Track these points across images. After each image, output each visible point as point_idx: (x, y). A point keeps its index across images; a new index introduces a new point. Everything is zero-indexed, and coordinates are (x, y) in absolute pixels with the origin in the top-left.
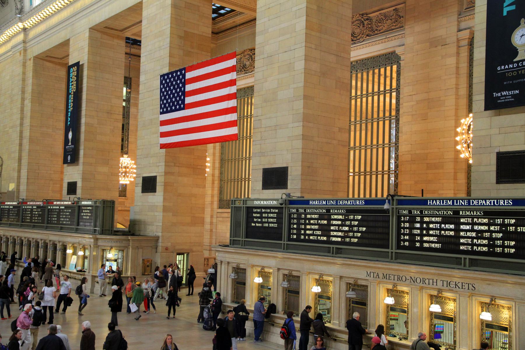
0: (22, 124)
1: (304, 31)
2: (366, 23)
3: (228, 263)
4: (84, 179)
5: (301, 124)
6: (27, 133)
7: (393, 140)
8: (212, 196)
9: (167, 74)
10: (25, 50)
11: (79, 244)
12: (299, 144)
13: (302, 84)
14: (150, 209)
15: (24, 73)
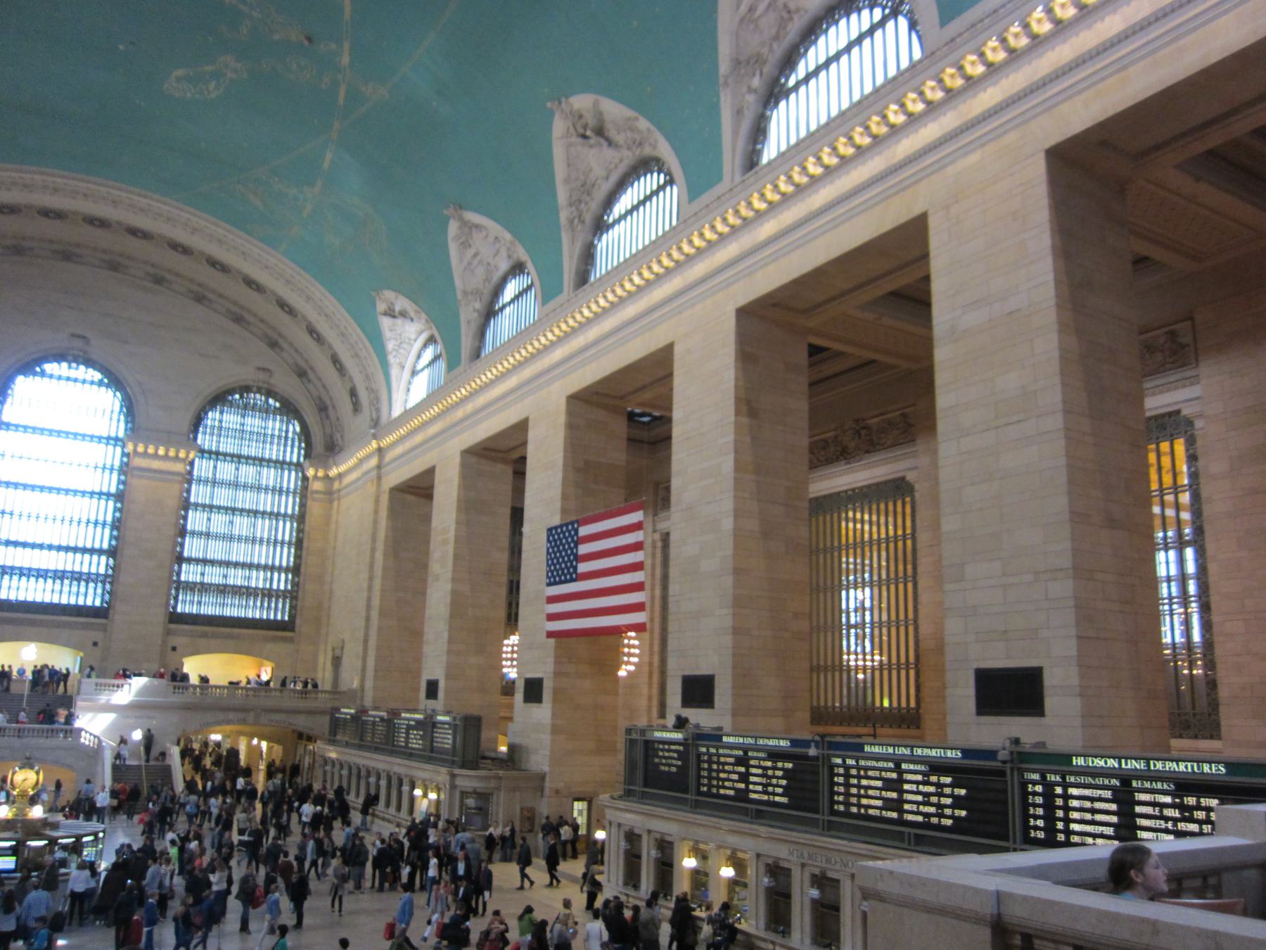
0: (370, 588)
1: (732, 475)
2: (863, 432)
3: (619, 825)
4: (447, 677)
5: (730, 611)
6: (376, 602)
7: (911, 616)
8: (650, 698)
9: (556, 528)
10: (379, 478)
11: (431, 781)
12: (728, 640)
13: (730, 552)
14: (532, 727)
15: (376, 512)
